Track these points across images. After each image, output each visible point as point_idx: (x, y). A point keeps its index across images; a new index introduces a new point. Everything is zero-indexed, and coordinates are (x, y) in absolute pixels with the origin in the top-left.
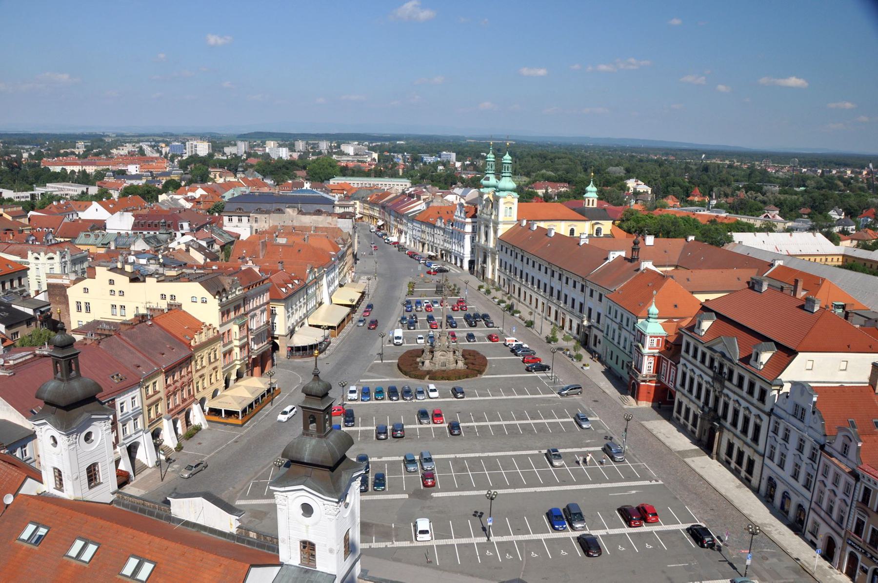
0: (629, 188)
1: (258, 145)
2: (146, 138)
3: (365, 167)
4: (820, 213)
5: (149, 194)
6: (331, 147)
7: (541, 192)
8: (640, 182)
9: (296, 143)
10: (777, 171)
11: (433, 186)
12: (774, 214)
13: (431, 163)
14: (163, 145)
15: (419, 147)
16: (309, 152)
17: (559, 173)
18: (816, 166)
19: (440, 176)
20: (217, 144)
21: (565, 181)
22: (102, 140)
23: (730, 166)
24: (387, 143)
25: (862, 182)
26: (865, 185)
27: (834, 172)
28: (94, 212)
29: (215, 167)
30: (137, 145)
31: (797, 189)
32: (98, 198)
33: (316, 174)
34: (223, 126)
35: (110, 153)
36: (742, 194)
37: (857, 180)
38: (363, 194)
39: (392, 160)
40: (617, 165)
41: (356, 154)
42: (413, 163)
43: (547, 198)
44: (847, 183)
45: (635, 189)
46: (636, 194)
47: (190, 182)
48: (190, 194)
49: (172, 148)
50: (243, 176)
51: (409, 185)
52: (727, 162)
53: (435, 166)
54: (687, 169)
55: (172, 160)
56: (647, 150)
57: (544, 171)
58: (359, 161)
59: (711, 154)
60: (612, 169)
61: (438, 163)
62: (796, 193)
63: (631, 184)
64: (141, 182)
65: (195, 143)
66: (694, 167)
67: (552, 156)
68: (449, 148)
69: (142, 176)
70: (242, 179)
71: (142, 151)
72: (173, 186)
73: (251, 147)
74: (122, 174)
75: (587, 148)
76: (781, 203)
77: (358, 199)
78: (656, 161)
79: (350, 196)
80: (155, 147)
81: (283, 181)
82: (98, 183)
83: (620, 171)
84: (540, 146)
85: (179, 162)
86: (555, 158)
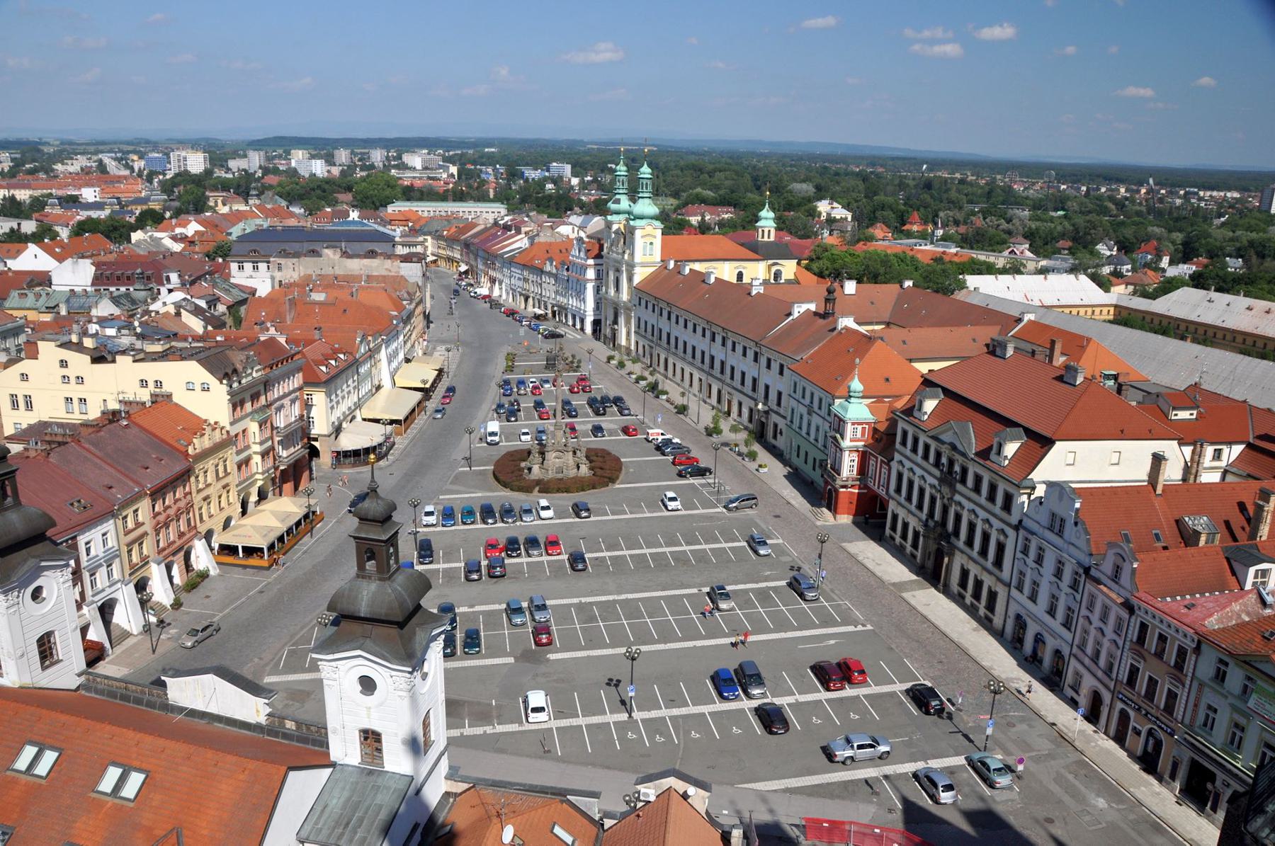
0: (820, 213)
1: (280, 157)
2: (108, 147)
3: (439, 186)
4: (1085, 247)
5: (116, 231)
6: (387, 158)
7: (694, 220)
8: (835, 205)
9: (336, 152)
10: (1026, 189)
11: (538, 212)
12: (1023, 250)
13: (532, 180)
14: (135, 158)
15: (515, 158)
16: (356, 166)
17: (722, 192)
18: (1078, 181)
19: (550, 197)
20: (218, 154)
21: (729, 204)
22: (39, 151)
23: (962, 182)
24: (471, 152)
25: (1140, 204)
26: (1144, 209)
27: (1103, 190)
28: (32, 259)
29: (216, 190)
30: (95, 158)
31: (1053, 214)
32: (36, 238)
33: (367, 198)
34: (225, 129)
35: (53, 170)
36: (978, 221)
37: (1133, 201)
38: (435, 226)
39: (479, 177)
40: (804, 181)
41: (425, 168)
42: (508, 180)
43: (704, 228)
44: (1121, 205)
45: (829, 214)
46: (831, 221)
47: (178, 213)
48: (178, 230)
49: (149, 161)
50: (258, 202)
51: (503, 211)
52: (958, 175)
53: (541, 183)
54: (902, 185)
55: (150, 179)
56: (843, 159)
57: (699, 190)
58: (430, 178)
59: (935, 164)
60: (797, 186)
61: (545, 180)
62: (1052, 220)
63: (823, 207)
64: (103, 214)
65: (183, 154)
66: (911, 183)
67: (711, 167)
68: (563, 158)
69: (105, 204)
70: (257, 207)
71: (102, 167)
72: (152, 218)
73: (269, 159)
74: (73, 201)
75: (761, 156)
76: (1032, 234)
77: (429, 233)
78: (858, 174)
79: (417, 229)
80: (123, 160)
81: (319, 209)
82: (35, 215)
83: (806, 188)
84: (693, 153)
85: (160, 181)
86: (715, 171)
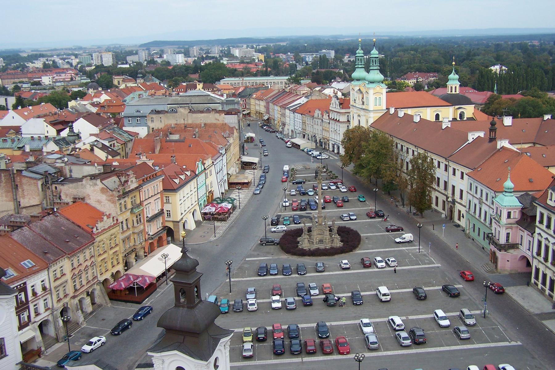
48: (95, 100)
50: (142, 81)
72: (81, 95)
